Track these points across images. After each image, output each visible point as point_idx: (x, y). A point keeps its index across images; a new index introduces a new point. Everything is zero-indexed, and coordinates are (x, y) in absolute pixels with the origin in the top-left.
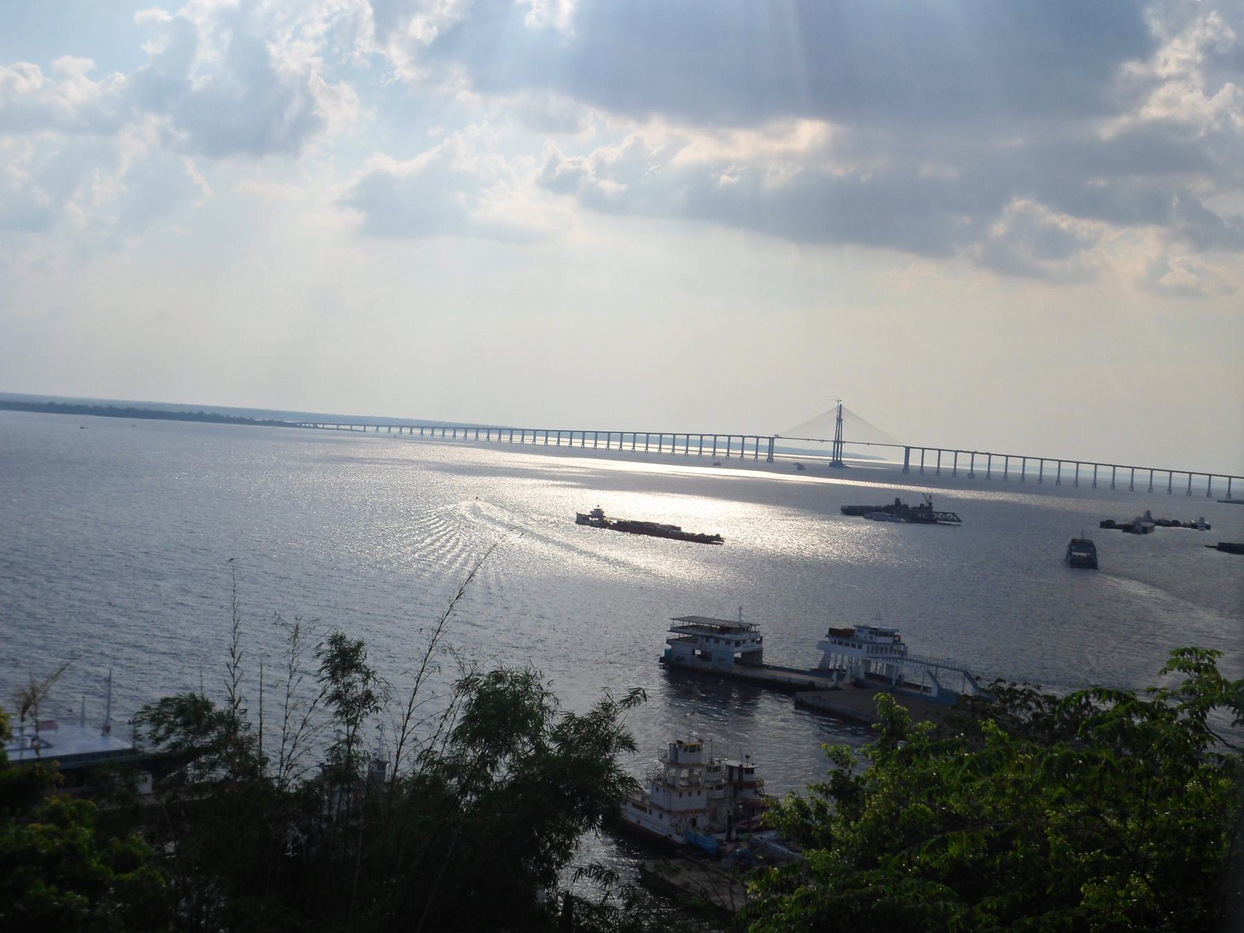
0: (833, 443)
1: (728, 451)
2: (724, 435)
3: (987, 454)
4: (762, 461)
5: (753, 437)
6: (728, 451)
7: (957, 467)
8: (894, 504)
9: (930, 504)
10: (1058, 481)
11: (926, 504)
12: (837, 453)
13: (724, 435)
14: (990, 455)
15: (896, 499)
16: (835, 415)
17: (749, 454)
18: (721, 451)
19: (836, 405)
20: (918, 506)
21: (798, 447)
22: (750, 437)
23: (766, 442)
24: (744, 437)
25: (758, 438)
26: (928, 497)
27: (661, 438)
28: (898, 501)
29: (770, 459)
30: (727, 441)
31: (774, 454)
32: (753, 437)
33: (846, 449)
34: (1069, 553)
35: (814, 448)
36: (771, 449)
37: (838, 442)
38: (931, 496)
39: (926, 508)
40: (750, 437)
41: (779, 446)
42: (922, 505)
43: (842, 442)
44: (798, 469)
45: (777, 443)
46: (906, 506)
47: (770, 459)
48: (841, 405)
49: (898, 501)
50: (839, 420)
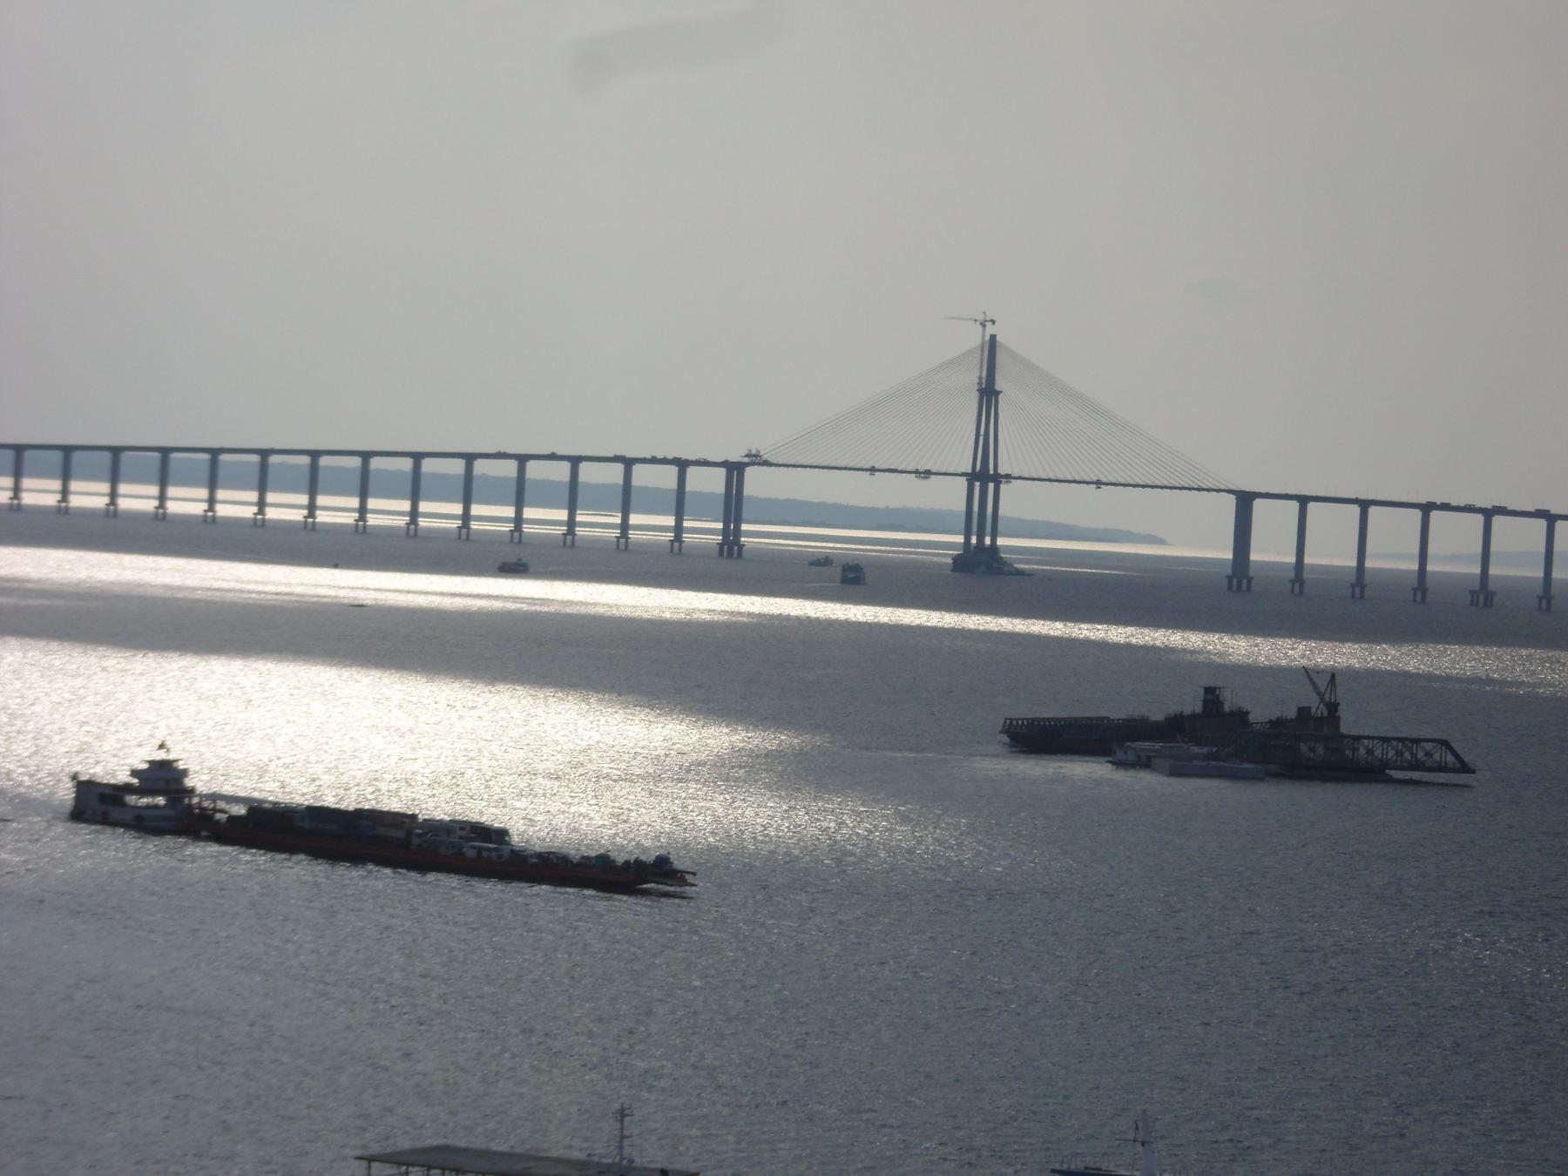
0: (963, 482)
1: (572, 515)
2: (553, 457)
4: (700, 552)
5: (664, 461)
6: (572, 515)
7: (1431, 567)
8: (1198, 708)
9: (1333, 707)
11: (1321, 711)
12: (981, 519)
13: (553, 457)
15: (1210, 691)
16: (971, 378)
17: (651, 525)
18: (545, 518)
19: (973, 338)
20: (1291, 713)
22: (654, 461)
23: (708, 482)
24: (629, 463)
25: (682, 465)
26: (1323, 684)
27: (314, 467)
28: (1212, 696)
29: (731, 545)
30: (620, 480)
31: (744, 527)
32: (664, 461)
33: (1014, 502)
35: (895, 503)
36: (733, 506)
37: (984, 477)
38: (1333, 676)
39: (1320, 721)
40: (654, 461)
42: (1303, 712)
43: (998, 479)
44: (845, 581)
45: (756, 483)
46: (1241, 716)
47: (731, 545)
48: (993, 338)
49: (1212, 696)
50: (988, 393)
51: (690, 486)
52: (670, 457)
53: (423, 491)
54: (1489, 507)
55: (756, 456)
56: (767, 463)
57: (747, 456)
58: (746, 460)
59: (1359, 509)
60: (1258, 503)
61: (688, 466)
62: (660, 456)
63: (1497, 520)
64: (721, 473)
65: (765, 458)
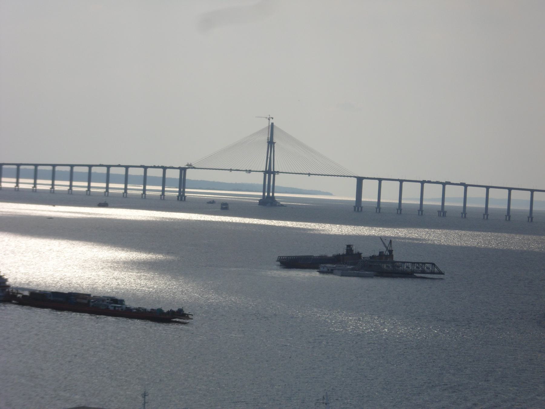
0: (262, 174)
1: (126, 186)
2: (119, 166)
4: (171, 199)
5: (158, 167)
6: (126, 186)
8: (345, 253)
9: (391, 252)
10: (531, 215)
11: (387, 253)
12: (269, 187)
13: (119, 166)
14: (466, 186)
15: (349, 246)
16: (265, 138)
17: (154, 189)
18: (117, 187)
19: (266, 124)
20: (377, 254)
21: (217, 180)
22: (155, 167)
23: (173, 174)
24: (146, 168)
25: (164, 168)
26: (387, 243)
27: (36, 170)
29: (182, 197)
30: (143, 174)
31: (186, 190)
32: (158, 167)
33: (280, 181)
36: (182, 183)
37: (270, 172)
38: (391, 241)
39: (387, 257)
40: (155, 167)
41: (193, 179)
42: (381, 253)
43: (274, 173)
44: (222, 208)
45: (190, 175)
46: (359, 255)
47: (182, 197)
48: (272, 124)
50: (271, 143)
51: (167, 176)
52: (160, 166)
53: (38, 175)
54: (444, 182)
55: (190, 165)
56: (194, 168)
57: (187, 165)
58: (187, 167)
61: (166, 169)
62: (157, 165)
63: (447, 186)
64: (178, 171)
65: (193, 166)
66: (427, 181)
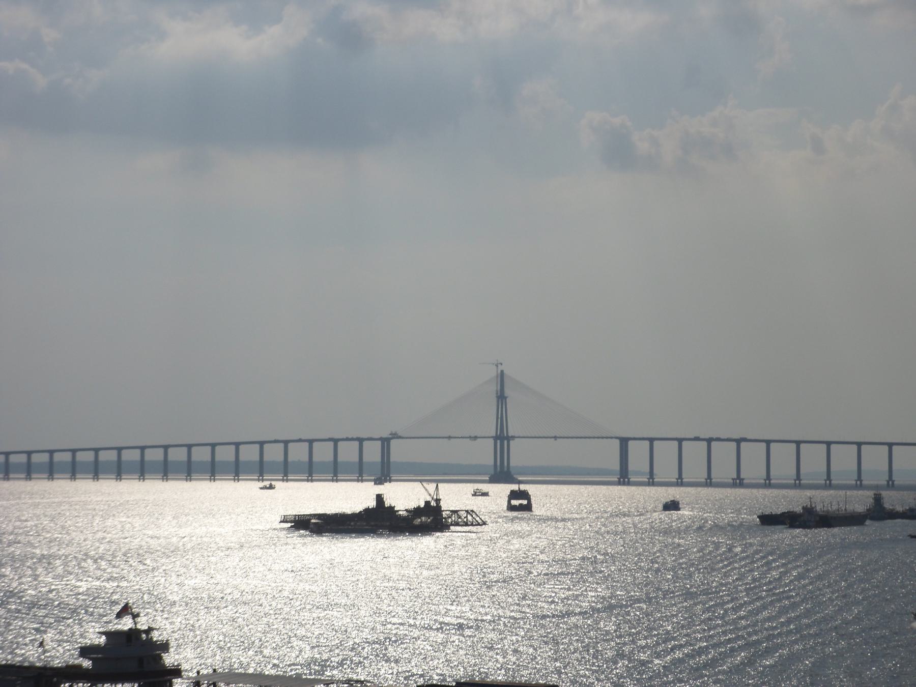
0: (492, 441)
3: (330, 440)
5: (352, 439)
19: (493, 372)
22: (347, 439)
32: (352, 439)
34: (509, 502)
40: (347, 439)
43: (509, 438)
48: (502, 371)
50: (501, 398)
52: (355, 437)
55: (395, 434)
56: (400, 437)
57: (390, 434)
58: (390, 436)
59: (649, 442)
60: (630, 443)
61: (364, 441)
62: (350, 437)
63: (743, 444)
65: (399, 435)
66: (714, 438)
